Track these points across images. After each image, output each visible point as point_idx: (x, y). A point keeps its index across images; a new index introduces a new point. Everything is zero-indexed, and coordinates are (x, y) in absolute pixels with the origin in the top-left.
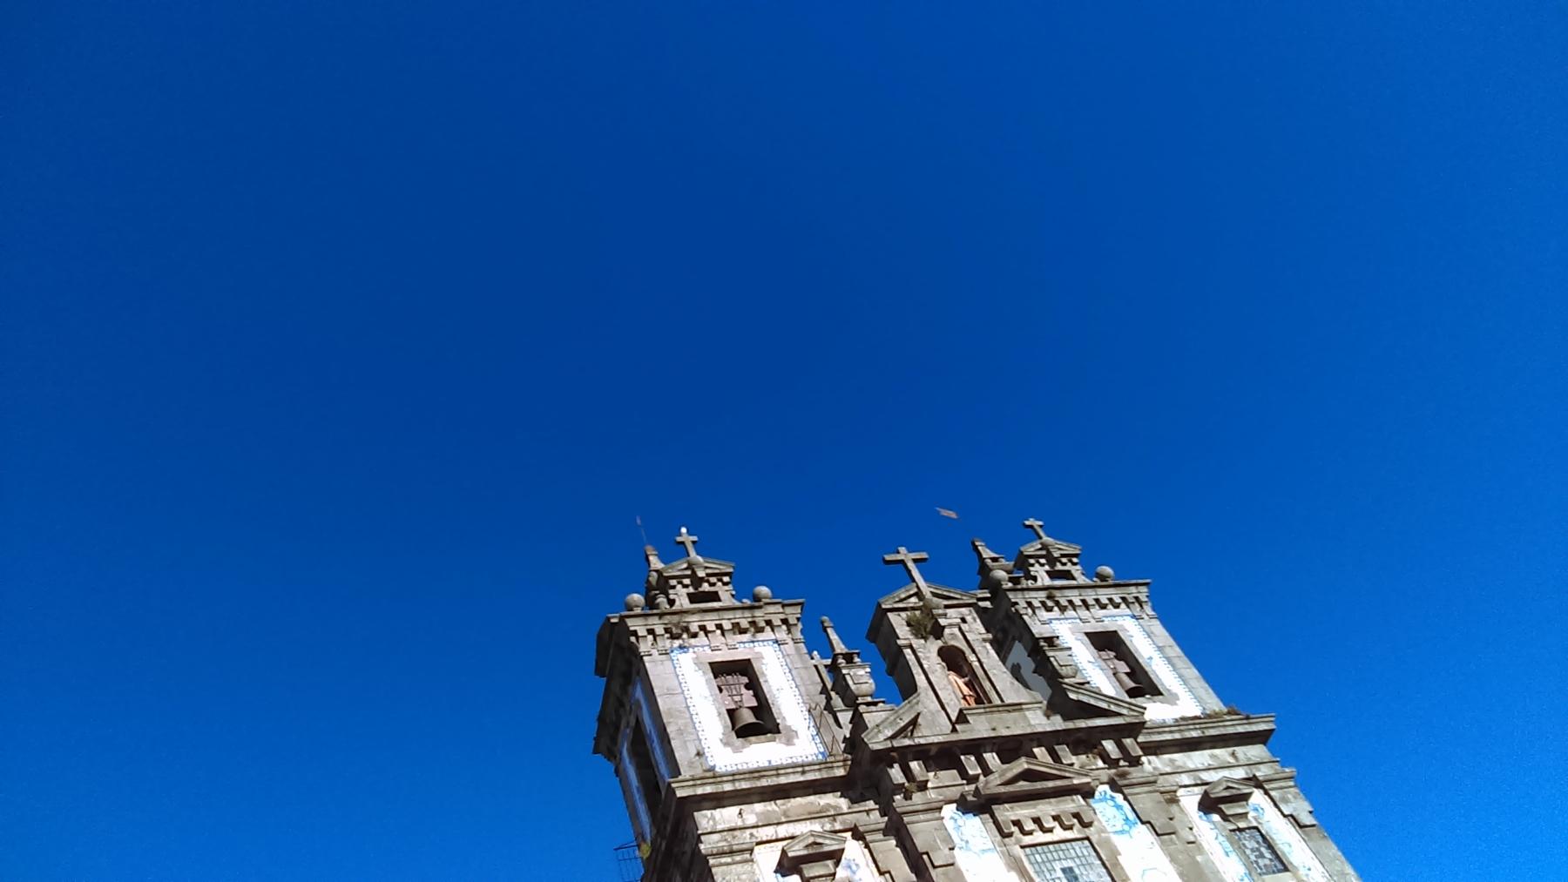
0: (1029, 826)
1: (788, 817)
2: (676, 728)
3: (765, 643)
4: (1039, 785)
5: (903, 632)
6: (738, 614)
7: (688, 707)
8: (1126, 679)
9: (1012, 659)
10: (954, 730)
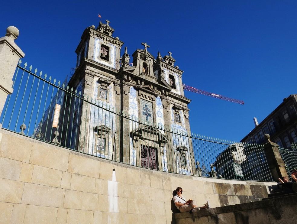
0: (144, 96)
4: (149, 91)
5: (139, 57)
6: (111, 39)
8: (171, 84)
9: (155, 73)
10: (139, 75)
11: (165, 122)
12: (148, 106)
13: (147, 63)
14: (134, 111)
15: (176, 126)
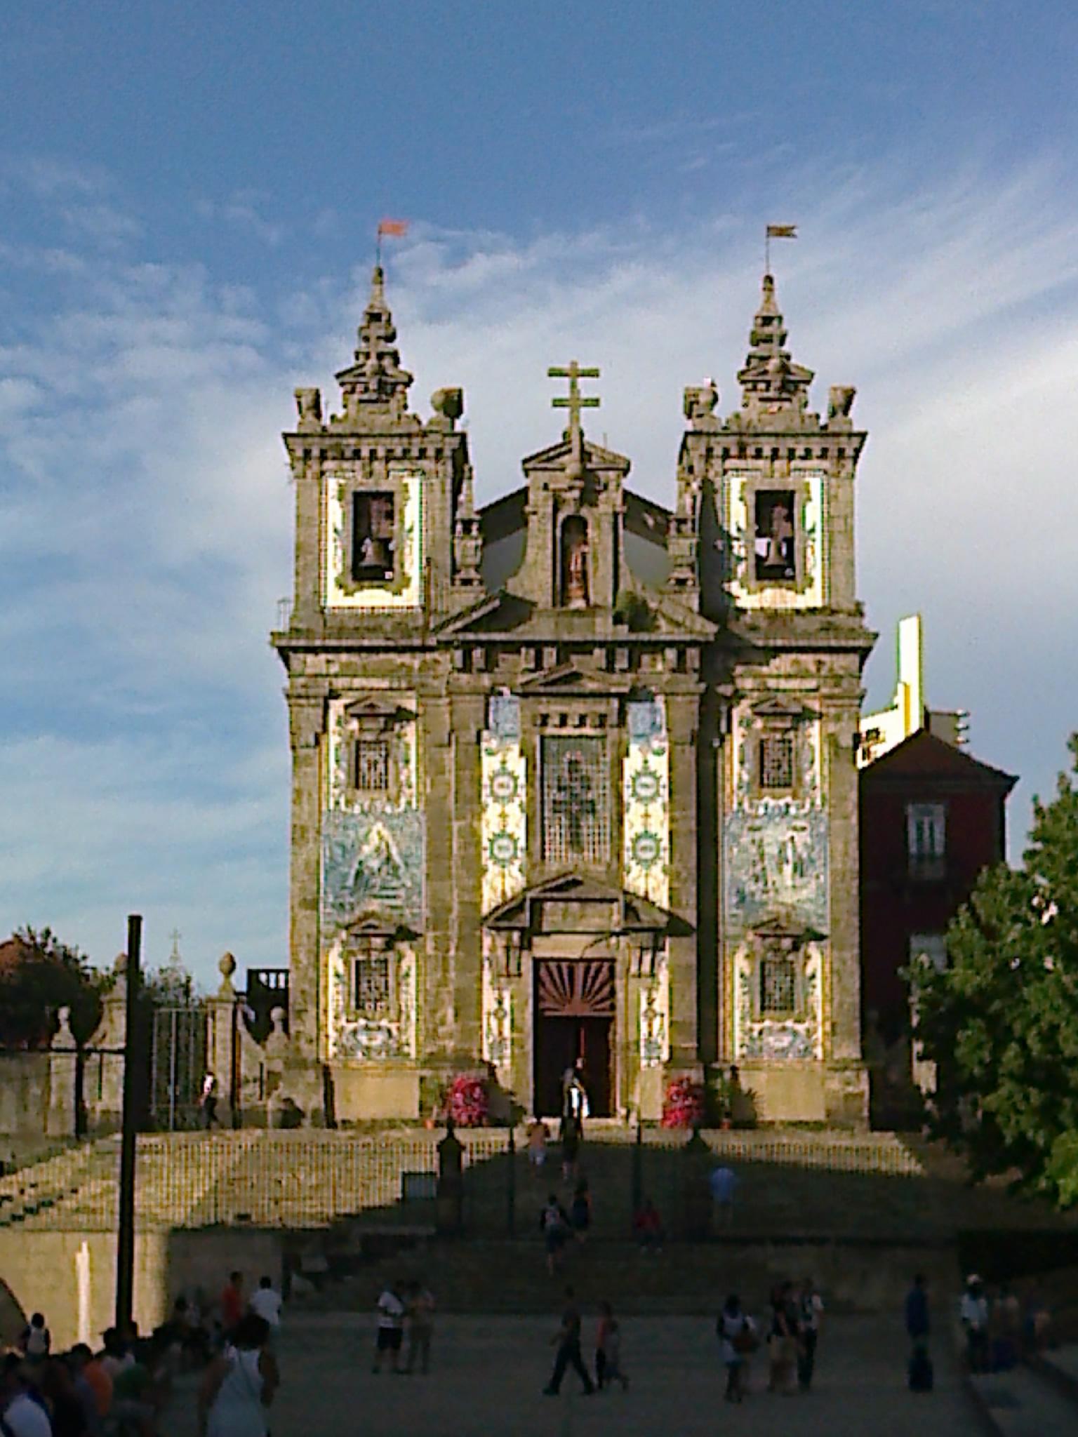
0: (557, 721)
6: (396, 440)
7: (320, 540)
11: (672, 820)
12: (583, 767)
13: (584, 512)
15: (761, 811)
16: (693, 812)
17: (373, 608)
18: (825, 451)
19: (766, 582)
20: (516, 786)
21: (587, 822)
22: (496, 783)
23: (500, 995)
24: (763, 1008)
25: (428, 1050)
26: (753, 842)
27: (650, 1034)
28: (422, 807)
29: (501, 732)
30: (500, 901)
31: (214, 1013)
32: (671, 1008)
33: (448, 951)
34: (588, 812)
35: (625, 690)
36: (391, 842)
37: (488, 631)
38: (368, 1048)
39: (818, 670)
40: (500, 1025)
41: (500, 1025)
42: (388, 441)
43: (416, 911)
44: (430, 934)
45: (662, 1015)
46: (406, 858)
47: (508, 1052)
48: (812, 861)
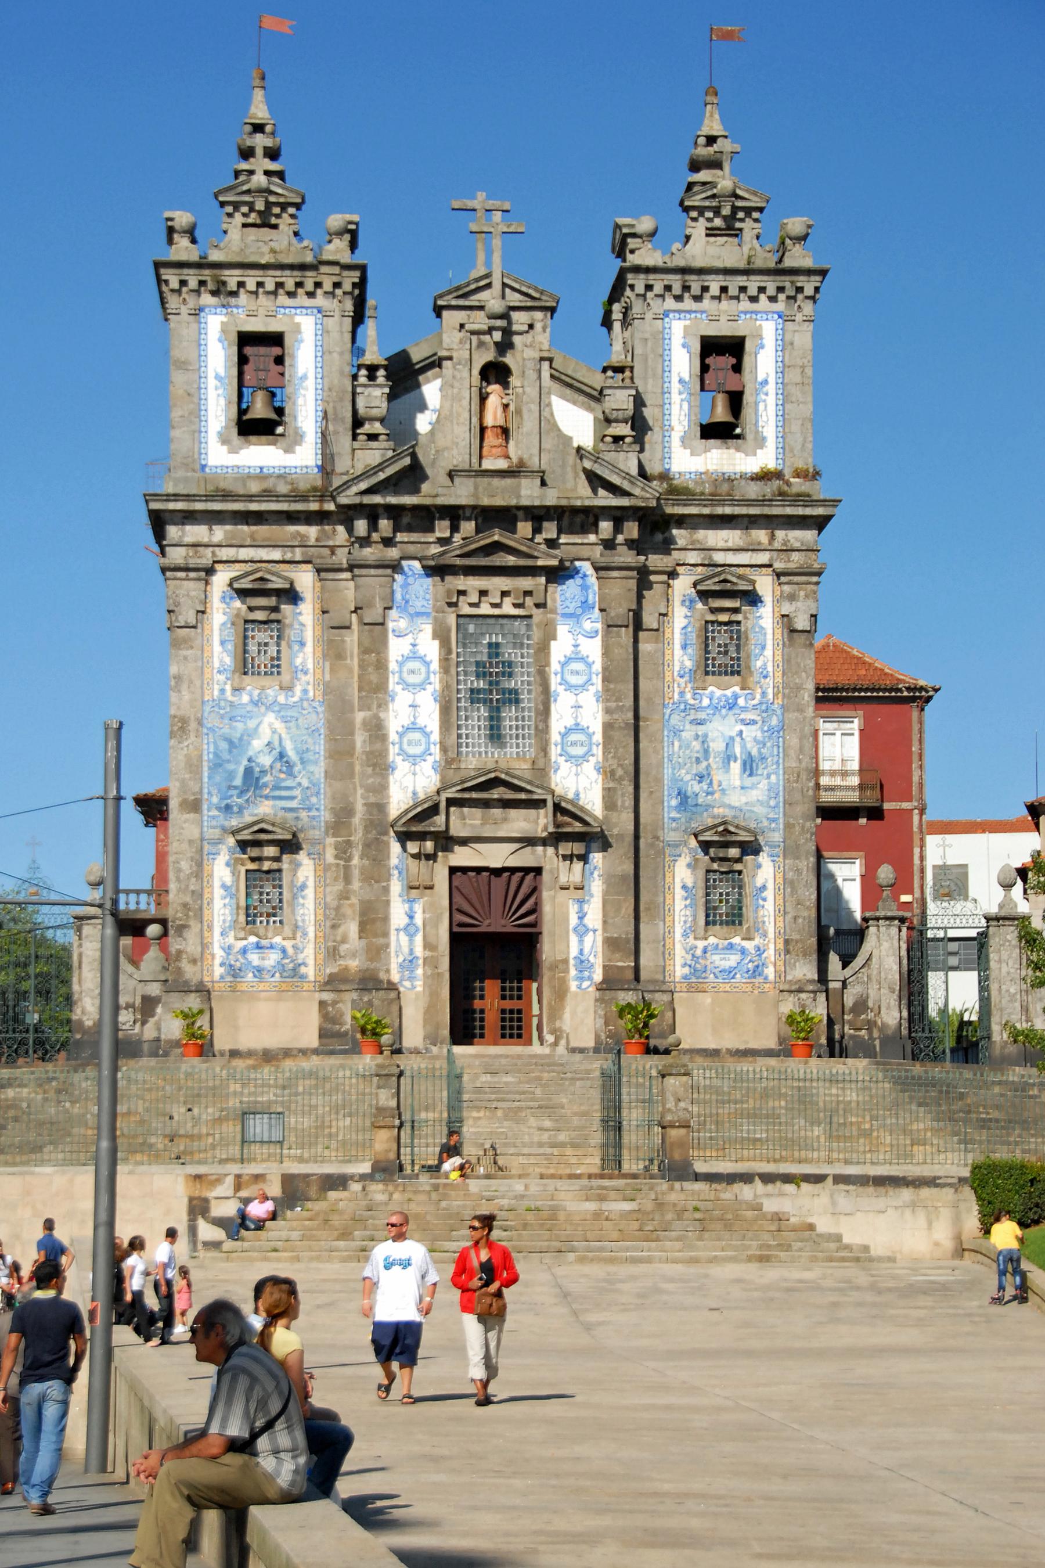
0: (474, 598)
1: (254, 540)
2: (180, 413)
3: (309, 311)
6: (288, 273)
7: (199, 388)
11: (608, 711)
14: (418, 702)
15: (706, 702)
16: (629, 702)
17: (261, 468)
18: (781, 289)
19: (712, 441)
20: (428, 672)
21: (509, 714)
22: (405, 669)
23: (411, 909)
24: (707, 923)
25: (328, 971)
26: (697, 737)
27: (581, 950)
28: (319, 693)
29: (412, 610)
30: (411, 803)
31: (79, 930)
32: (605, 922)
33: (349, 859)
34: (510, 701)
35: (555, 562)
36: (284, 736)
37: (396, 493)
38: (259, 970)
39: (770, 544)
40: (411, 941)
41: (411, 941)
42: (278, 273)
43: (314, 813)
44: (330, 841)
45: (595, 931)
46: (302, 753)
47: (420, 971)
48: (763, 759)
